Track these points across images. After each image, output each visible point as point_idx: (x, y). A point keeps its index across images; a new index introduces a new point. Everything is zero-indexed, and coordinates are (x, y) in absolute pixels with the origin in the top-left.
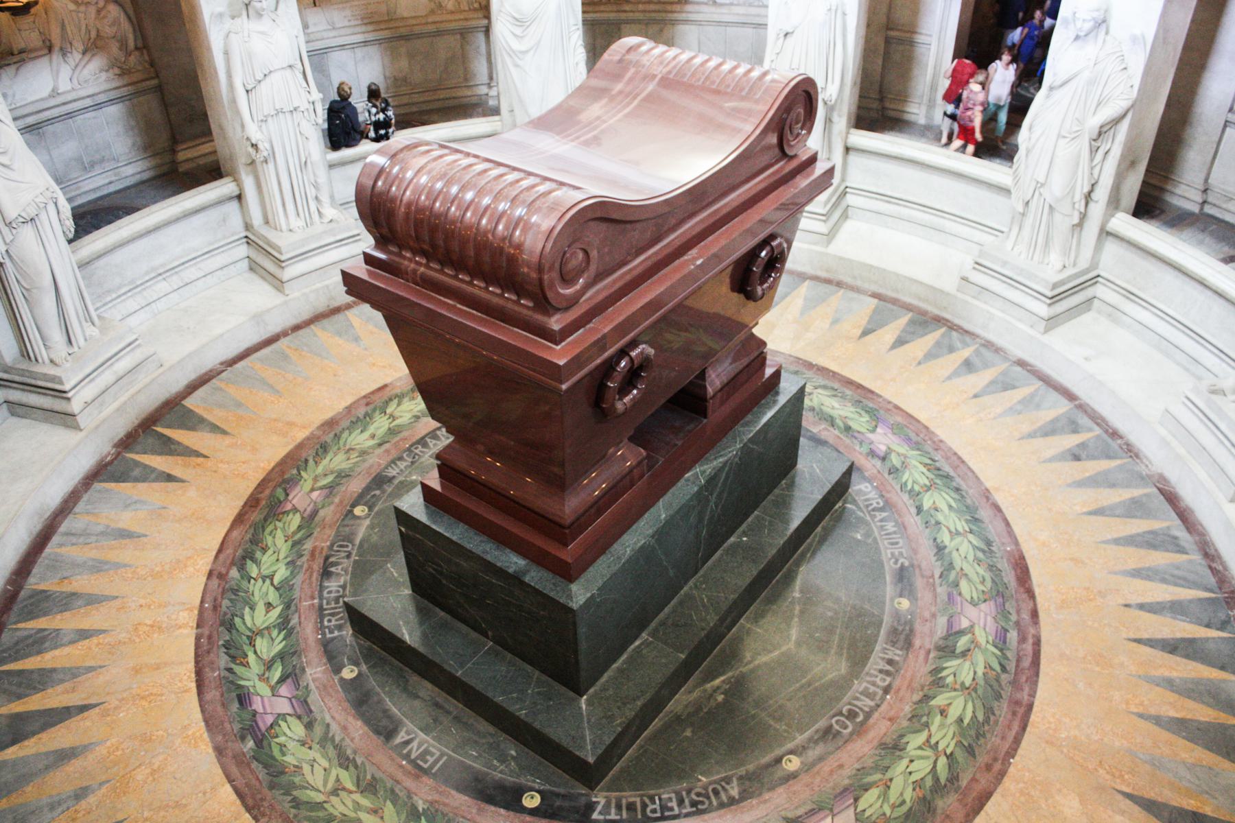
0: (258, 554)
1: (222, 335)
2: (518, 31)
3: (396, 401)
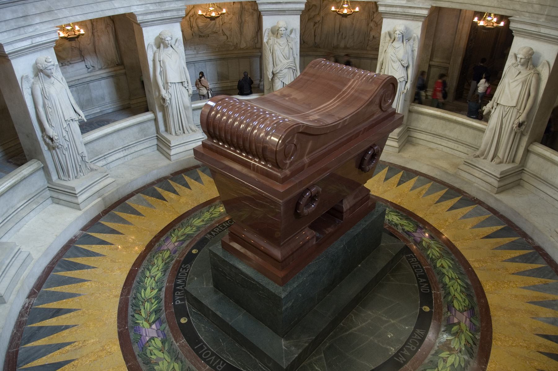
0: (463, 289)
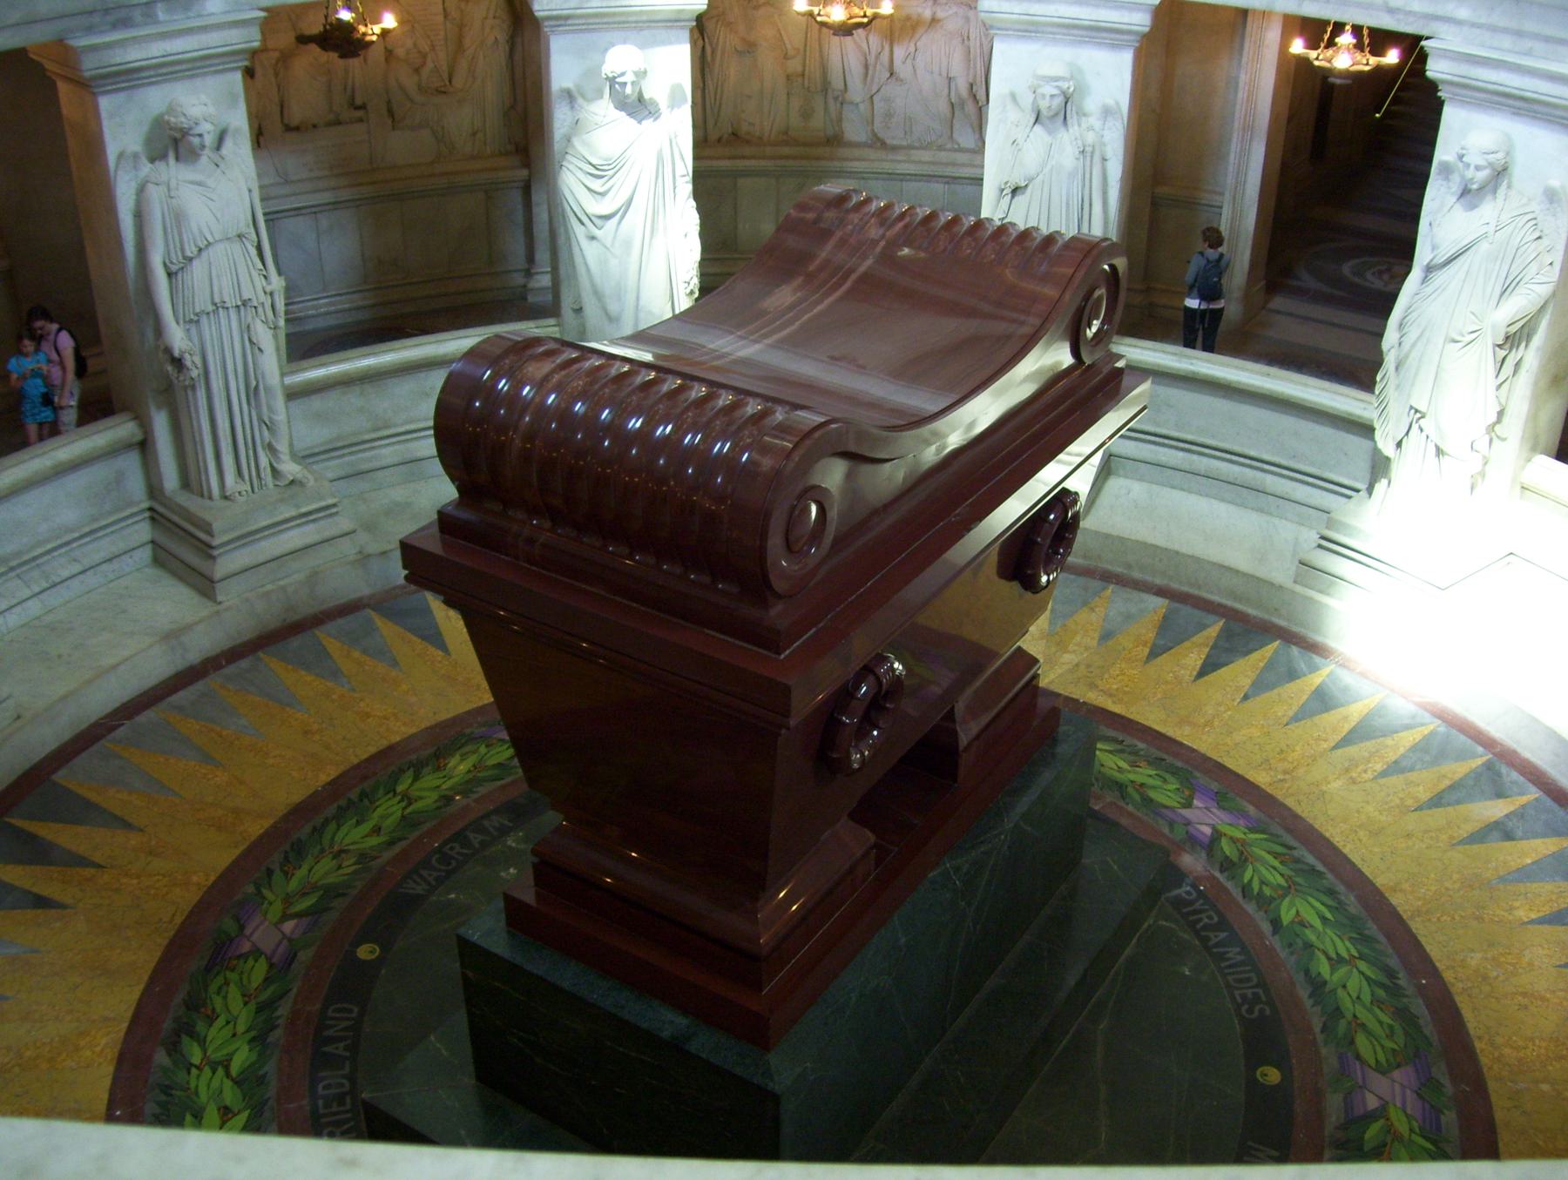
0: (200, 1027)
1: (114, 667)
2: (596, 185)
3: (410, 774)
